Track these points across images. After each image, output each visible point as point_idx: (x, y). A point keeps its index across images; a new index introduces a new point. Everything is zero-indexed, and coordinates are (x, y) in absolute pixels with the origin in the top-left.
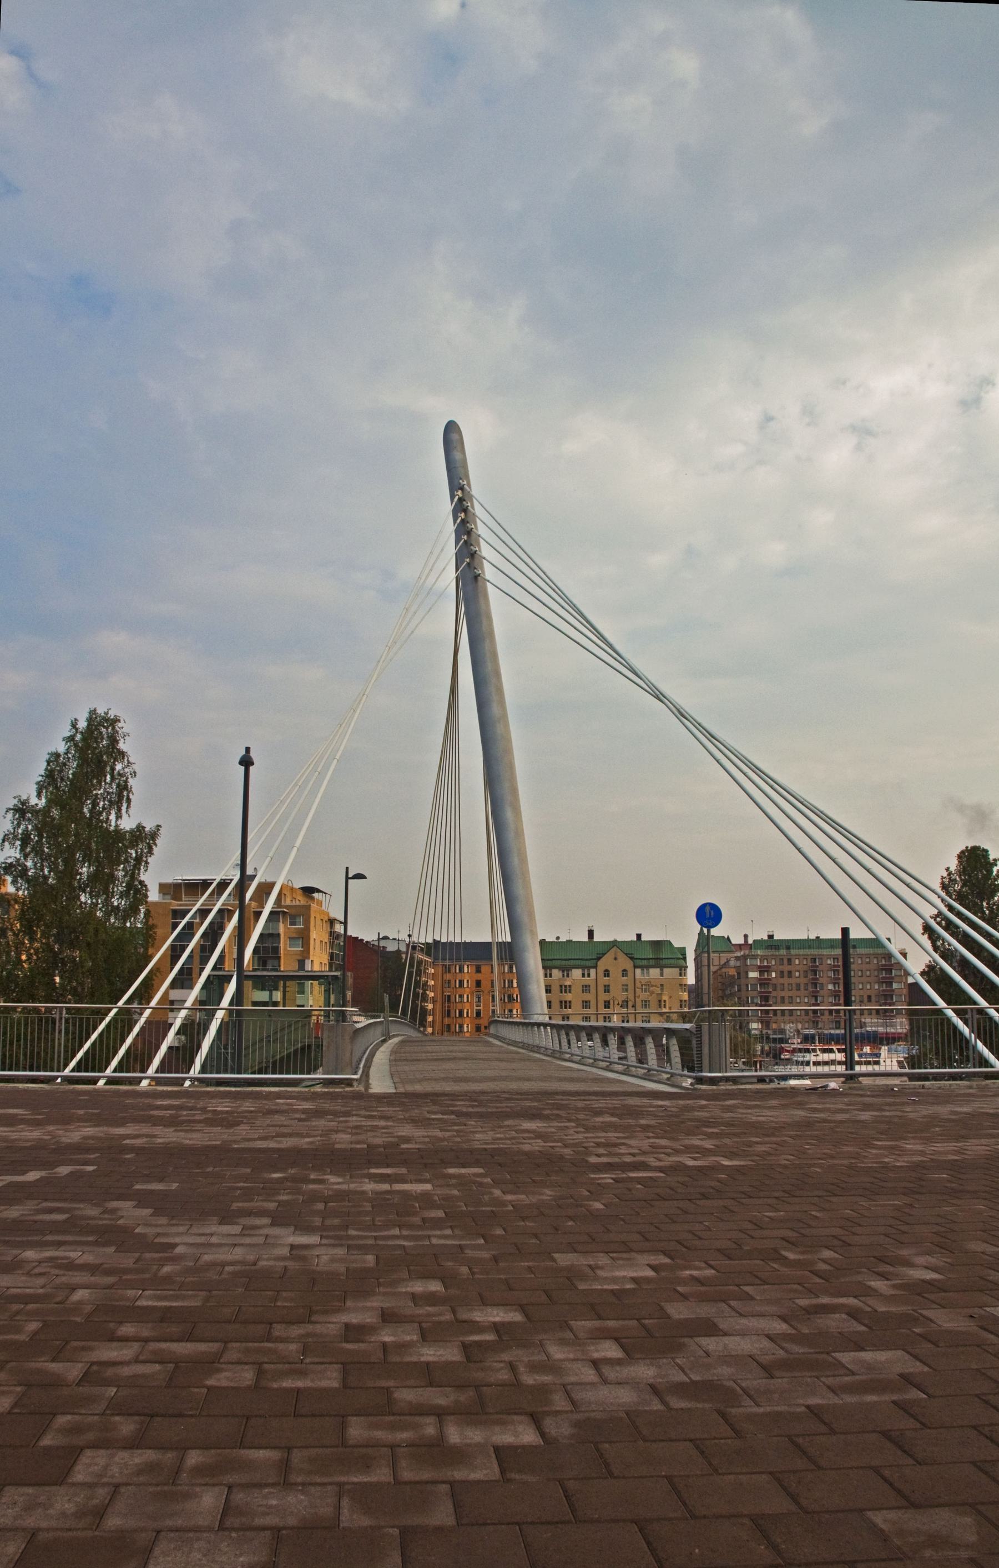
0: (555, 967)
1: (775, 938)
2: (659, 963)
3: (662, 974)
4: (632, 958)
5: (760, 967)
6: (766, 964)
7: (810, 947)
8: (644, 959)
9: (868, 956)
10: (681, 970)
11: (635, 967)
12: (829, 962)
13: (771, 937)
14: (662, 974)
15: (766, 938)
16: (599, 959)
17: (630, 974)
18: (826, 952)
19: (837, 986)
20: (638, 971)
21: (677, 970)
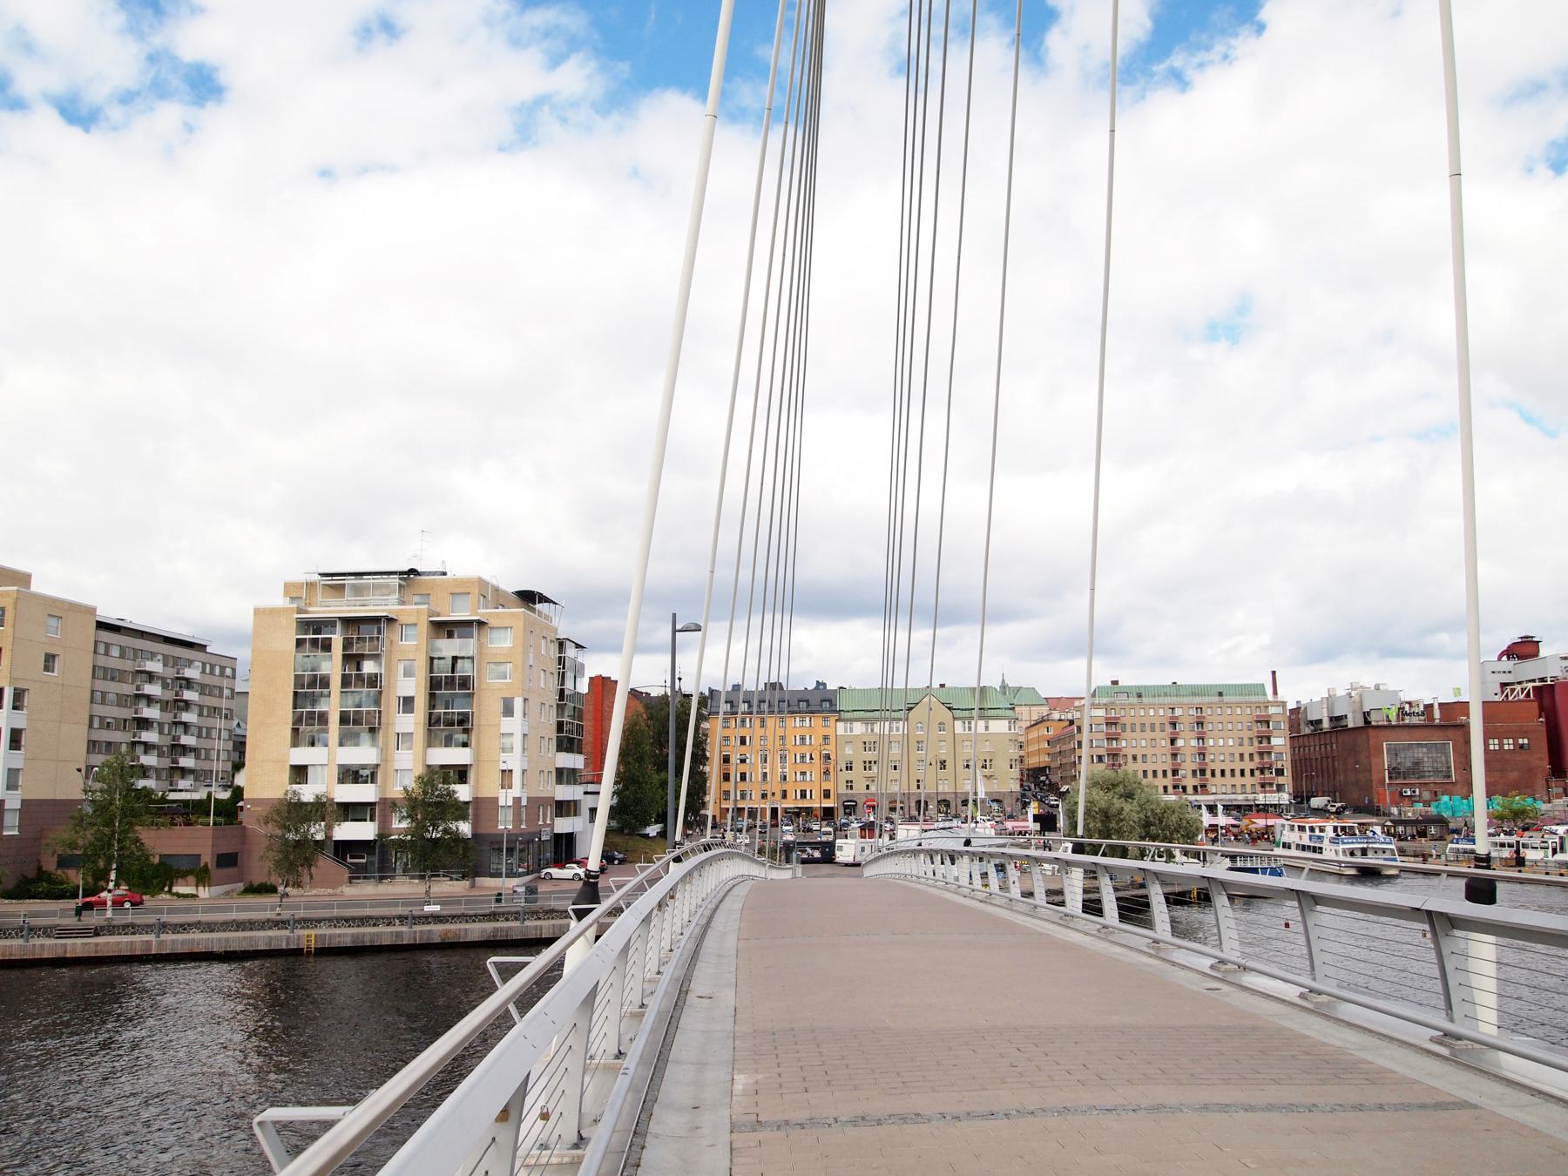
0: (857, 720)
1: (1120, 683)
2: (985, 713)
3: (987, 728)
4: (949, 708)
5: (1107, 718)
6: (1113, 715)
7: (1165, 695)
8: (966, 710)
9: (1239, 705)
10: (1010, 722)
11: (955, 719)
12: (1191, 713)
13: (1115, 683)
14: (987, 728)
15: (1110, 684)
16: (910, 709)
17: (948, 726)
18: (1186, 700)
19: (1201, 741)
20: (958, 724)
21: (1007, 722)
